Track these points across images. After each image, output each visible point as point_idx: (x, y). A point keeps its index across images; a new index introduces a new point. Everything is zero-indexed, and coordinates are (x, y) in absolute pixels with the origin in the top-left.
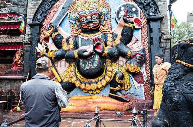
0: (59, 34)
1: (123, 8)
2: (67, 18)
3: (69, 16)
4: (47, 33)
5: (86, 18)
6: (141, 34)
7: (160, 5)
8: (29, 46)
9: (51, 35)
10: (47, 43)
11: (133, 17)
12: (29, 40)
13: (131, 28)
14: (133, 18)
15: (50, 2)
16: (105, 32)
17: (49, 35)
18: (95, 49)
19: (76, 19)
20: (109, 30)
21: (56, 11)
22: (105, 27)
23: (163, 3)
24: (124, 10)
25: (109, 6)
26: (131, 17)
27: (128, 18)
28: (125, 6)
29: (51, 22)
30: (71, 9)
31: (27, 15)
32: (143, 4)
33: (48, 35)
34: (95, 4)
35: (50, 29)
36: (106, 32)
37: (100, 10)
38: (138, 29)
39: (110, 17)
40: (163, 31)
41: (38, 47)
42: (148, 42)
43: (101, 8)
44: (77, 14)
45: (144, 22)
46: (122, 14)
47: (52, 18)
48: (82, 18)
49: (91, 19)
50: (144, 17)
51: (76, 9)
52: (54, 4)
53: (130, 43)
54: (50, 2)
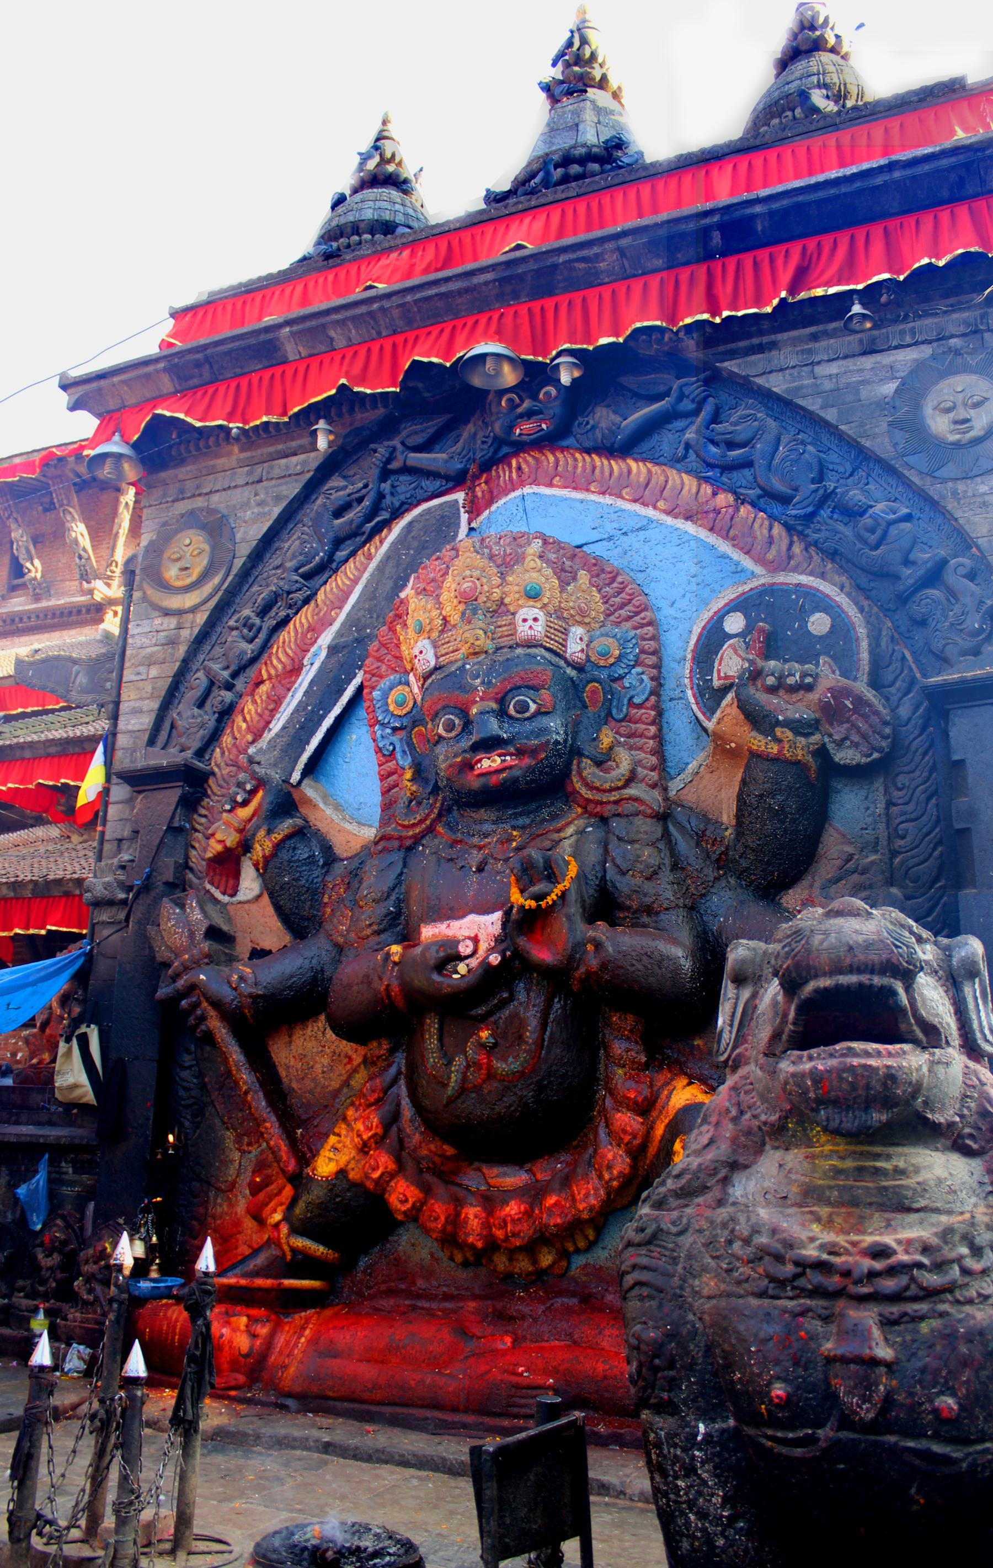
0: (301, 833)
1: (734, 624)
2: (362, 713)
4: (224, 834)
6: (890, 804)
10: (226, 899)
11: (808, 680)
14: (809, 688)
16: (608, 810)
20: (631, 791)
21: (291, 671)
22: (607, 771)
26: (790, 681)
27: (772, 690)
29: (251, 750)
31: (123, 707)
32: (896, 577)
33: (228, 844)
34: (529, 612)
35: (245, 803)
36: (616, 802)
37: (574, 648)
39: (655, 692)
42: (941, 868)
43: (577, 631)
47: (268, 723)
48: (437, 714)
52: (285, 622)
54: (263, 612)
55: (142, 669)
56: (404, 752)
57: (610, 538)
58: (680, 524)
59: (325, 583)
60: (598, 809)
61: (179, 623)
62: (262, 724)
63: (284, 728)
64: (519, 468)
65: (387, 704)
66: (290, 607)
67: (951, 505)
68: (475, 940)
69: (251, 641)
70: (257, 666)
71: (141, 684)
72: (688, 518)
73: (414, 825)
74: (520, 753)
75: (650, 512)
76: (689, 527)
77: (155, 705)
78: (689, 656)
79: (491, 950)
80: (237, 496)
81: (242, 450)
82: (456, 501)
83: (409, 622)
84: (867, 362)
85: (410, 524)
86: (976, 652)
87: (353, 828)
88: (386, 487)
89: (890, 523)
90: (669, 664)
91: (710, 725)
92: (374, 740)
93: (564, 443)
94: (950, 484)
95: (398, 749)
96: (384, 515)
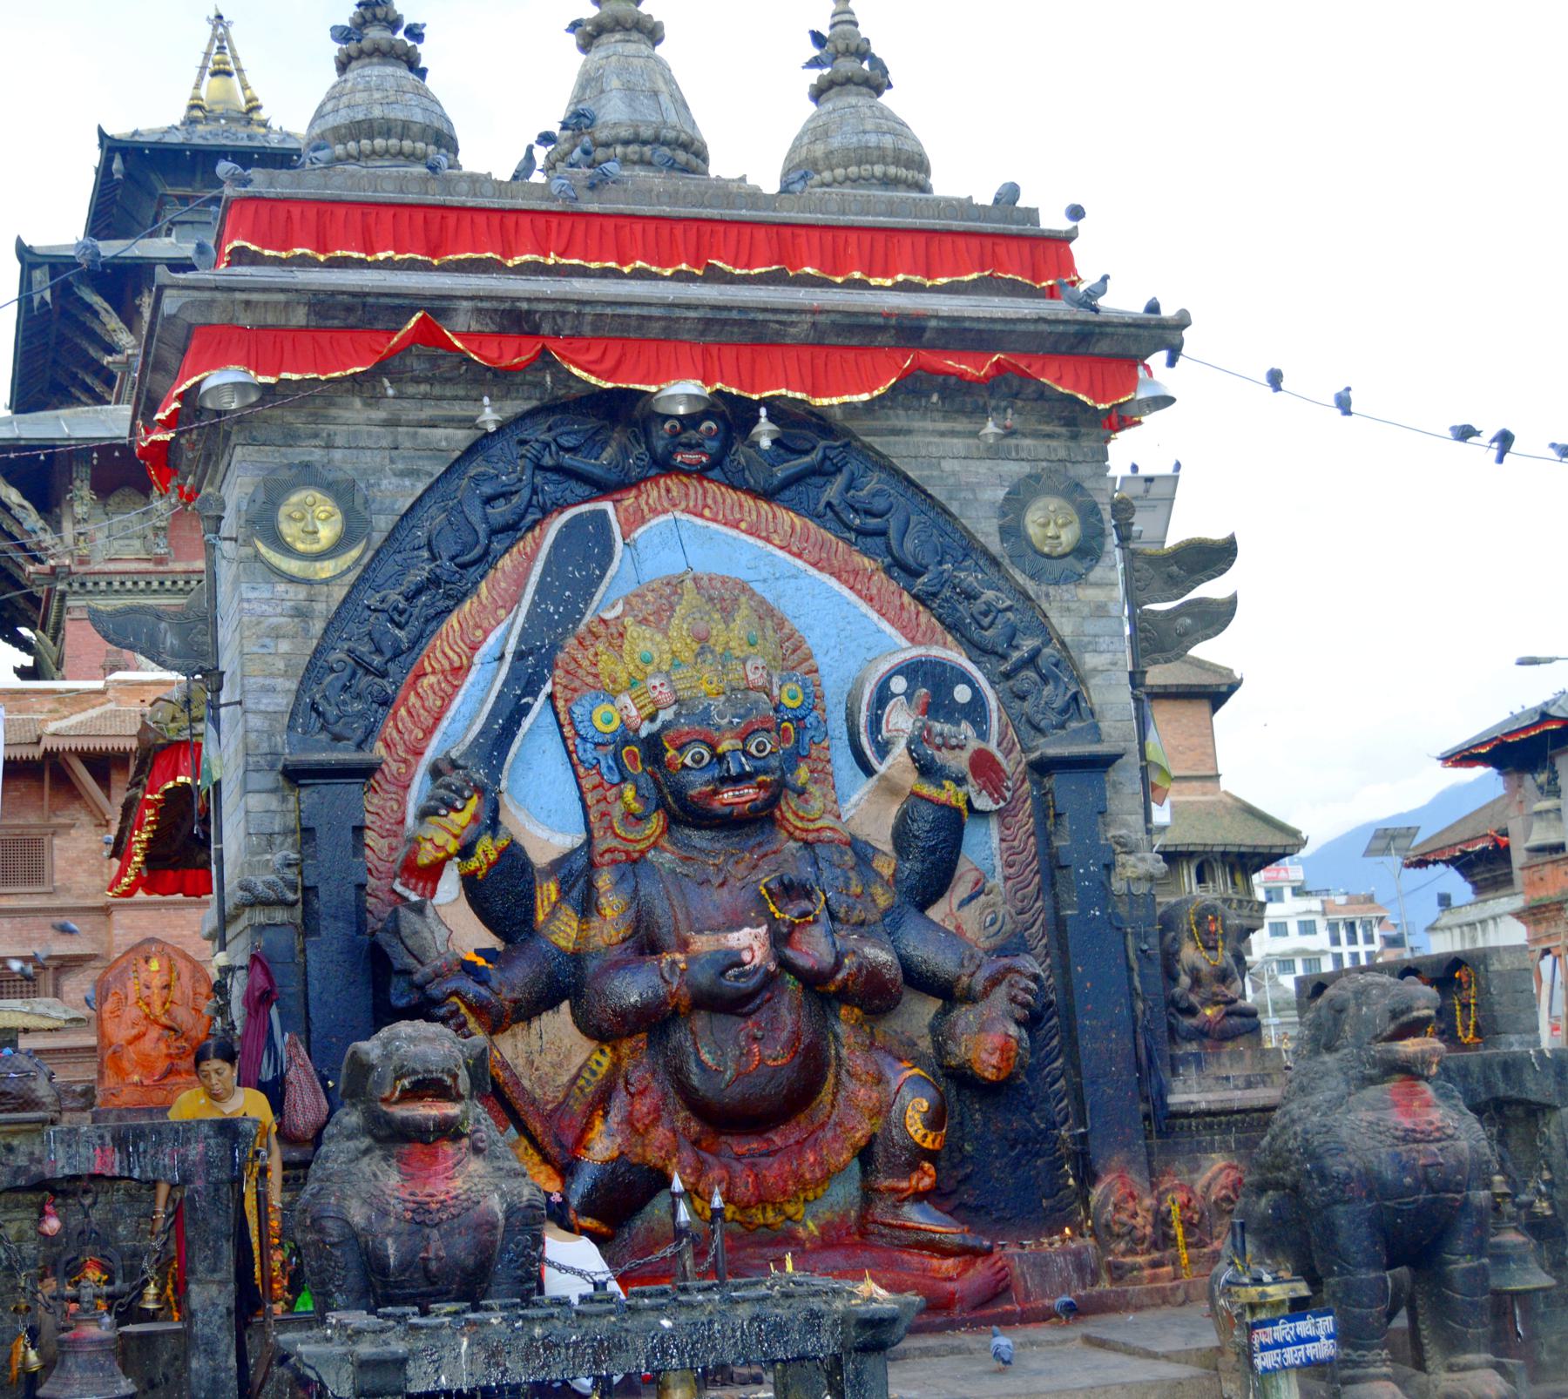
1: (899, 684)
3: (570, 711)
4: (441, 836)
5: (712, 747)
6: (1002, 840)
7: (1095, 670)
8: (280, 915)
9: (466, 852)
12: (291, 874)
13: (958, 810)
14: (961, 747)
15: (407, 599)
16: (810, 837)
17: (453, 846)
18: (789, 953)
19: (627, 743)
21: (460, 668)
23: (1107, 658)
24: (909, 695)
25: (809, 656)
26: (954, 742)
27: (938, 748)
28: (911, 670)
30: (573, 665)
35: (457, 811)
36: (818, 830)
37: (776, 692)
38: (984, 814)
40: (1123, 832)
41: (396, 932)
44: (634, 713)
45: (1012, 765)
46: (901, 720)
49: (746, 753)
50: (1011, 731)
51: (623, 678)
53: (947, 894)
54: (410, 598)
55: (267, 641)
56: (610, 768)
57: (765, 581)
58: (825, 577)
59: (482, 577)
60: (804, 835)
61: (309, 594)
62: (431, 721)
63: (482, 733)
64: (668, 491)
65: (591, 720)
66: (447, 596)
67: (1045, 606)
68: (751, 948)
69: (400, 626)
70: (413, 655)
71: (269, 659)
72: (832, 574)
73: (637, 841)
74: (761, 786)
75: (799, 562)
76: (833, 583)
77: (293, 685)
78: (864, 708)
79: (764, 958)
80: (368, 459)
81: (367, 405)
82: (605, 513)
83: (626, 647)
84: (983, 467)
85: (566, 526)
86: (1062, 726)
87: (542, 833)
88: (538, 480)
89: (1000, 611)
90: (830, 707)
91: (881, 769)
92: (569, 753)
93: (711, 474)
94: (1044, 588)
95: (603, 763)
96: (538, 516)
